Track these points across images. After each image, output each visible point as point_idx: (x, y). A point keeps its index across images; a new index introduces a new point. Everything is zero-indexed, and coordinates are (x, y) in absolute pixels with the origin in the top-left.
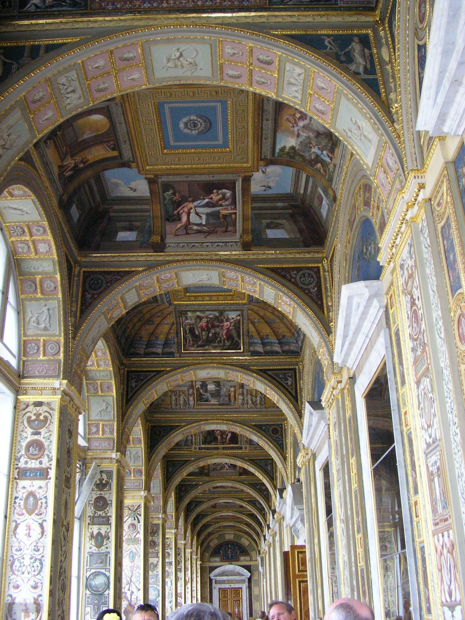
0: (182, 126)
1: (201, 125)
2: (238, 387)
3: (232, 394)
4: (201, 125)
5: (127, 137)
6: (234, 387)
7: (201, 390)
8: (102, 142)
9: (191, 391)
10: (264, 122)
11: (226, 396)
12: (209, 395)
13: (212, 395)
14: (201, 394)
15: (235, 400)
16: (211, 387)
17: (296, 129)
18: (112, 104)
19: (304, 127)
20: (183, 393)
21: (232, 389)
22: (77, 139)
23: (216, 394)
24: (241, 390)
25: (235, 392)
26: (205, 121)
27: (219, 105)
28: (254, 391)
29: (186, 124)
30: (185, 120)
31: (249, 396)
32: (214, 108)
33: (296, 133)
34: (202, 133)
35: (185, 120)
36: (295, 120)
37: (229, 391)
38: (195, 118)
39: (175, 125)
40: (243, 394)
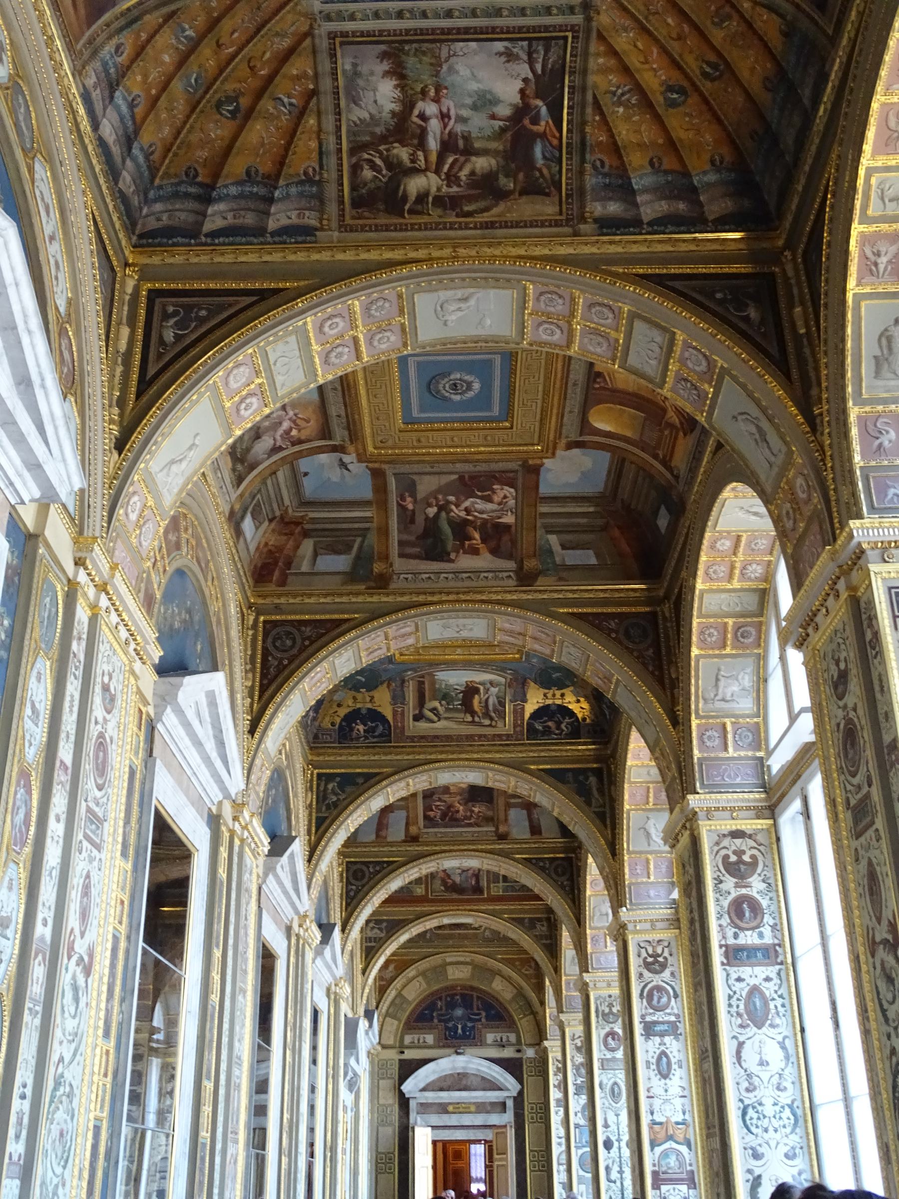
0: (476, 386)
1: (444, 387)
4: (444, 386)
5: (569, 391)
8: (614, 391)
10: (343, 414)
17: (291, 413)
18: (574, 437)
19: (280, 423)
22: (645, 419)
26: (438, 392)
27: (415, 414)
29: (469, 386)
30: (470, 394)
32: (422, 409)
33: (288, 408)
34: (444, 375)
35: (470, 394)
36: (297, 425)
38: (453, 397)
39: (487, 386)
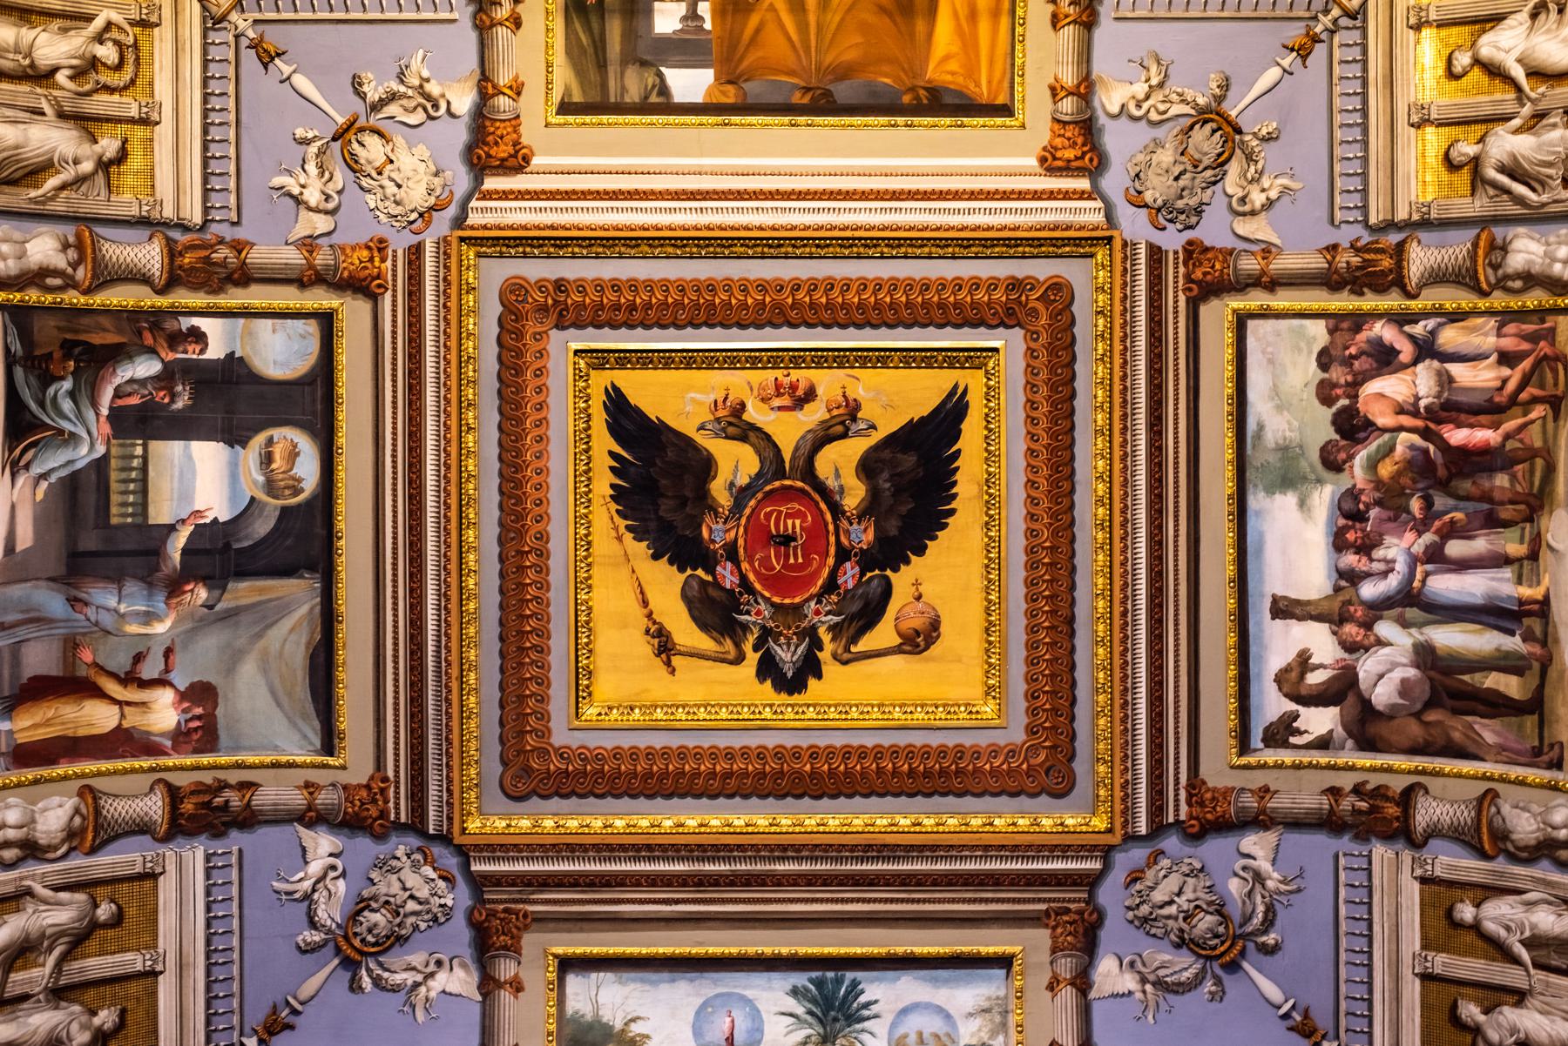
2: (186, 767)
3: (99, 717)
6: (201, 732)
7: (146, 368)
9: (149, 255)
11: (71, 645)
12: (83, 455)
13: (79, 497)
14: (94, 361)
15: (25, 755)
16: (201, 481)
20: (105, 166)
21: (163, 712)
23: (97, 538)
24: (154, 807)
25: (123, 742)
28: (135, 961)
31: (62, 915)
37: (130, 679)
40: (95, 831)
